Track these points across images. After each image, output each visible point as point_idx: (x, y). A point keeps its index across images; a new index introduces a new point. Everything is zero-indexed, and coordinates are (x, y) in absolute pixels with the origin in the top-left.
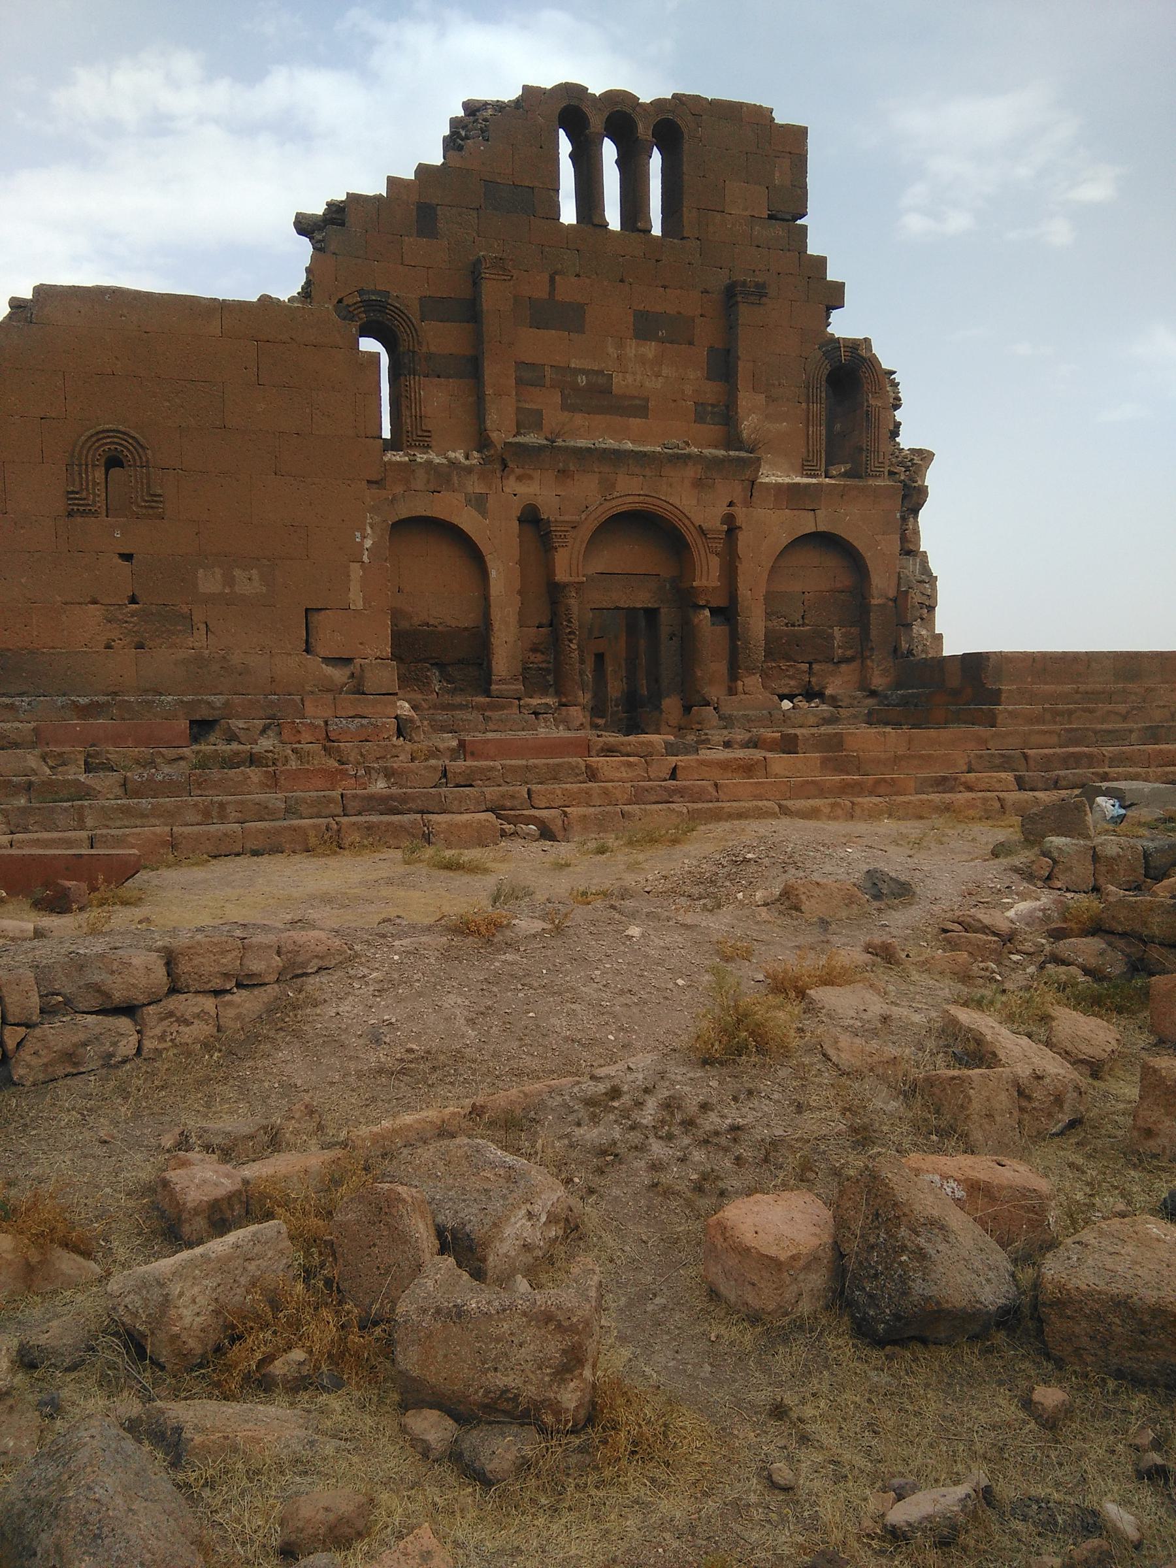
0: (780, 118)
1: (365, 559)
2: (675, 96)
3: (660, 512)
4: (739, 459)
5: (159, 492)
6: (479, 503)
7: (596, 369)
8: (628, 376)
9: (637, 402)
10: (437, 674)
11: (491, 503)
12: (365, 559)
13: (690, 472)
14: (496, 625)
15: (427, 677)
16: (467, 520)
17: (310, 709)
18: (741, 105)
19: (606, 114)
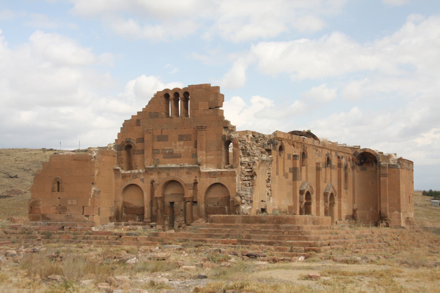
0: (212, 86)
1: (91, 197)
2: (188, 86)
3: (178, 181)
4: (195, 167)
5: (63, 187)
6: (143, 180)
7: (170, 148)
8: (177, 149)
9: (179, 155)
10: (138, 217)
11: (145, 180)
12: (91, 197)
13: (185, 171)
14: (145, 207)
15: (135, 218)
16: (140, 184)
17: (78, 225)
18: (202, 85)
19: (173, 93)
